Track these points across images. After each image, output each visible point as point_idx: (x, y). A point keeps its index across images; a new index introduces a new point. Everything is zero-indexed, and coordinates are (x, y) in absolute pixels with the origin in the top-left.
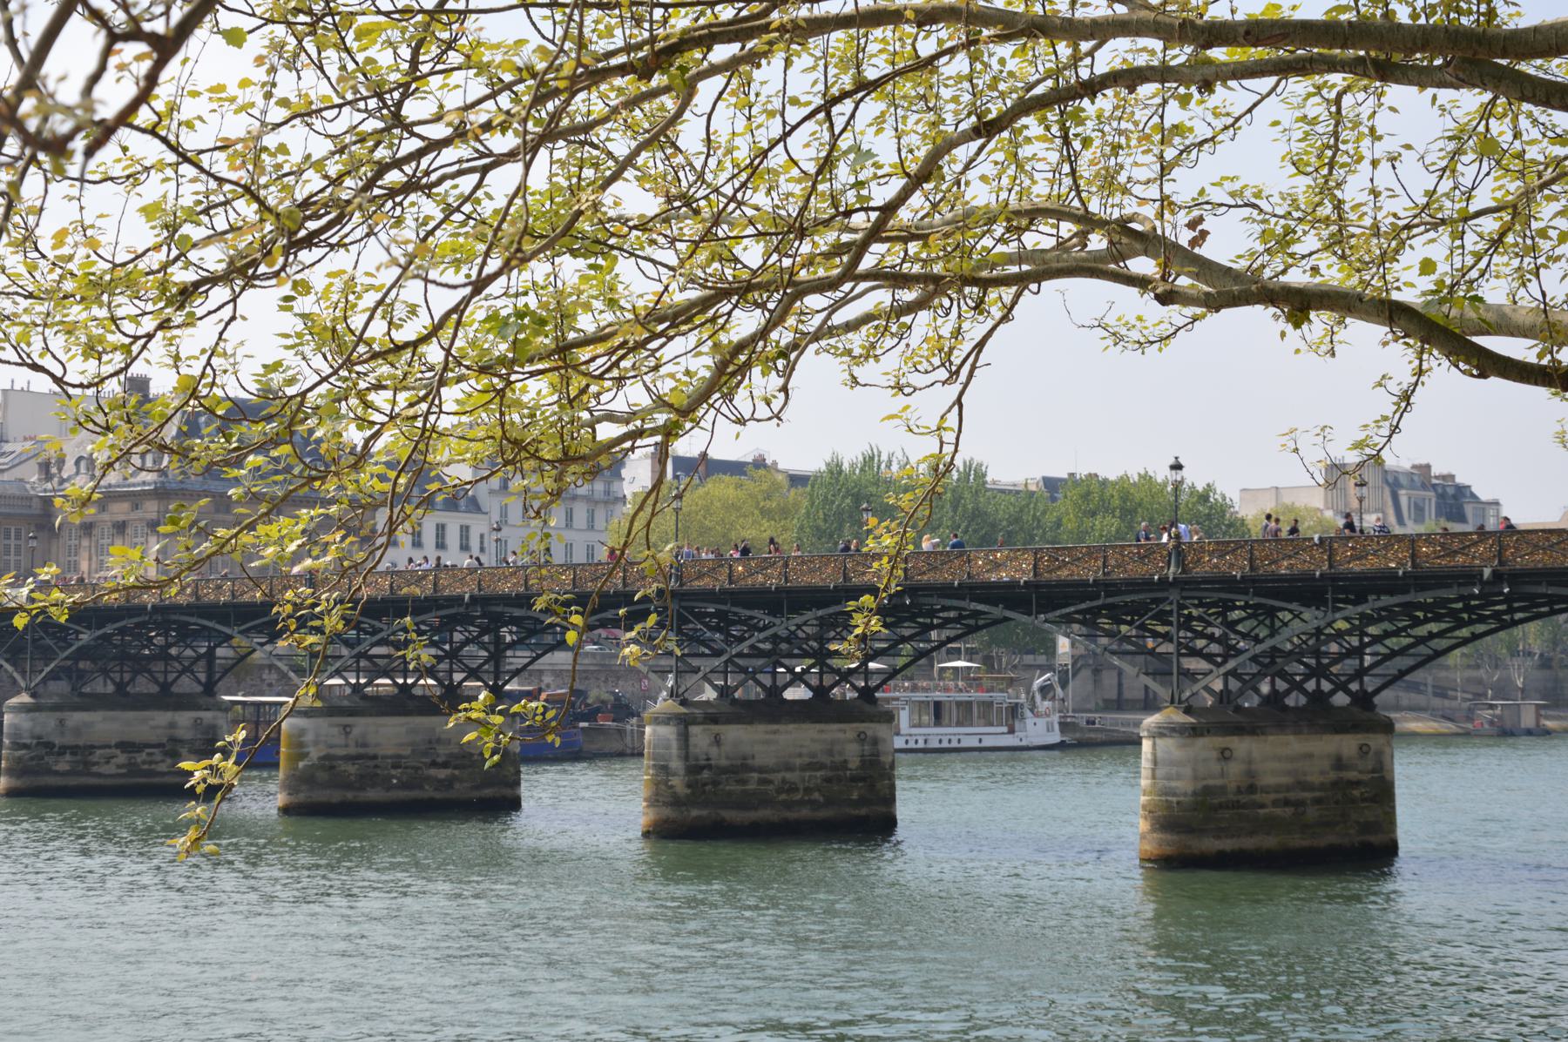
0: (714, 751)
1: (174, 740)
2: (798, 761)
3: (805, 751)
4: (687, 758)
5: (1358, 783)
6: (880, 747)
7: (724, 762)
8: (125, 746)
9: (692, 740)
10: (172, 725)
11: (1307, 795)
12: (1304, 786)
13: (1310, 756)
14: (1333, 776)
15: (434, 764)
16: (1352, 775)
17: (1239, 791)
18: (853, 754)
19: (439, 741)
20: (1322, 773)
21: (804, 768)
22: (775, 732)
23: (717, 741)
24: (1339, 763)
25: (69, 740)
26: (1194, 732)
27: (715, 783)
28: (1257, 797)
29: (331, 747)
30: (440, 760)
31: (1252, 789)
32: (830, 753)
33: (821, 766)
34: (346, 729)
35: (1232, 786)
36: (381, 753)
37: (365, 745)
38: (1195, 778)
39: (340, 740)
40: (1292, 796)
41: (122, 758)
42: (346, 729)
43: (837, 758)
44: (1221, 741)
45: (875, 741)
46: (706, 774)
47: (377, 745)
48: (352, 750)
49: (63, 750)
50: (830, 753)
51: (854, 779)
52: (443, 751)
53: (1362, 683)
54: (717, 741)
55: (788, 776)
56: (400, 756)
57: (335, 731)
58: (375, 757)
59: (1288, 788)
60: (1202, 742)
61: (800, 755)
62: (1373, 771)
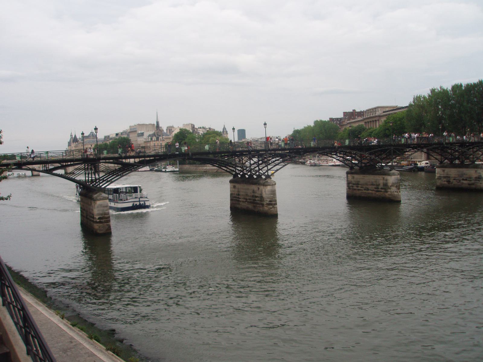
0: (352, 180)
2: (369, 183)
3: (370, 181)
6: (388, 181)
7: (354, 183)
9: (349, 177)
14: (252, 194)
15: (463, 180)
16: (257, 195)
18: (381, 182)
19: (464, 174)
20: (250, 193)
22: (364, 177)
23: (353, 178)
24: (254, 192)
27: (353, 187)
29: (441, 174)
30: (465, 179)
32: (376, 182)
33: (375, 185)
34: (444, 171)
36: (451, 176)
37: (448, 174)
39: (442, 173)
42: (444, 171)
43: (378, 183)
44: (234, 184)
45: (387, 180)
46: (351, 185)
47: (450, 174)
48: (445, 176)
50: (376, 182)
53: (268, 173)
54: (353, 178)
55: (367, 187)
56: (455, 177)
57: (441, 171)
58: (449, 177)
61: (369, 182)
62: (260, 194)
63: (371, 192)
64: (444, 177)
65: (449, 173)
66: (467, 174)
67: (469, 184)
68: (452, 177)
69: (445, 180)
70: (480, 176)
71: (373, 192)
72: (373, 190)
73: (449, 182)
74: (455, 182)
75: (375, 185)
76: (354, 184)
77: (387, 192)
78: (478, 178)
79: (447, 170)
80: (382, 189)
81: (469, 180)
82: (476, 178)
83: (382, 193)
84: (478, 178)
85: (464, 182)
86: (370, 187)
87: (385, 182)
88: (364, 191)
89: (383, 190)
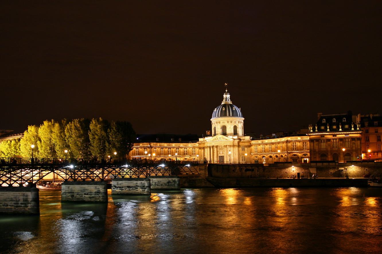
1: (137, 186)
8: (129, 187)
10: (137, 183)
15: (85, 194)
19: (86, 190)
25: (119, 186)
30: (86, 193)
32: (16, 198)
33: (14, 201)
36: (75, 191)
37: (72, 190)
41: (128, 189)
47: (74, 190)
48: (69, 191)
52: (86, 192)
55: (6, 202)
56: (78, 192)
58: (74, 192)
63: (9, 207)
64: (69, 193)
65: (73, 189)
66: (88, 190)
67: (90, 198)
68: (76, 192)
69: (69, 195)
70: (99, 190)
71: (13, 207)
72: (13, 206)
73: (73, 196)
74: (78, 196)
75: (14, 201)
77: (27, 207)
78: (98, 192)
79: (71, 186)
80: (21, 204)
81: (89, 195)
82: (95, 192)
83: (22, 208)
84: (98, 192)
85: (86, 196)
86: (9, 203)
87: (25, 197)
88: (3, 207)
89: (23, 205)
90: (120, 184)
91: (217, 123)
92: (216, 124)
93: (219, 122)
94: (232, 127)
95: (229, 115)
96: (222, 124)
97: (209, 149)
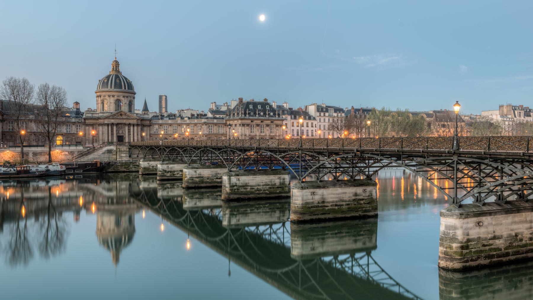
0: (238, 182)
2: (262, 184)
4: (230, 184)
5: (363, 199)
7: (240, 184)
9: (231, 180)
11: (344, 203)
12: (343, 201)
13: (346, 193)
14: (354, 198)
17: (319, 203)
21: (263, 186)
24: (356, 195)
25: (169, 170)
26: (302, 188)
27: (238, 189)
28: (326, 204)
31: (323, 202)
32: (271, 182)
33: (269, 185)
35: (317, 202)
38: (303, 200)
39: (195, 174)
40: (338, 203)
43: (273, 183)
44: (312, 190)
45: (284, 179)
46: (235, 187)
48: (197, 176)
49: (168, 172)
50: (271, 182)
51: (277, 188)
55: (259, 187)
59: (337, 202)
60: (305, 191)
76: (241, 186)
90: (171, 168)
91: (109, 96)
92: (107, 97)
93: (113, 96)
94: (128, 103)
95: (125, 88)
96: (116, 98)
97: (106, 127)
